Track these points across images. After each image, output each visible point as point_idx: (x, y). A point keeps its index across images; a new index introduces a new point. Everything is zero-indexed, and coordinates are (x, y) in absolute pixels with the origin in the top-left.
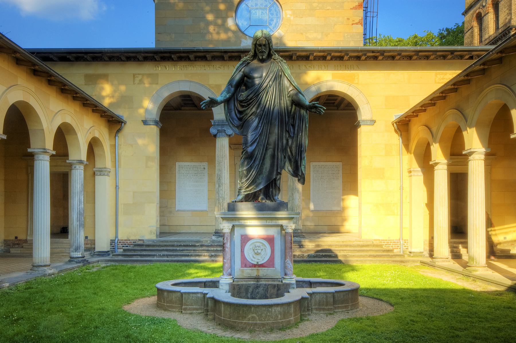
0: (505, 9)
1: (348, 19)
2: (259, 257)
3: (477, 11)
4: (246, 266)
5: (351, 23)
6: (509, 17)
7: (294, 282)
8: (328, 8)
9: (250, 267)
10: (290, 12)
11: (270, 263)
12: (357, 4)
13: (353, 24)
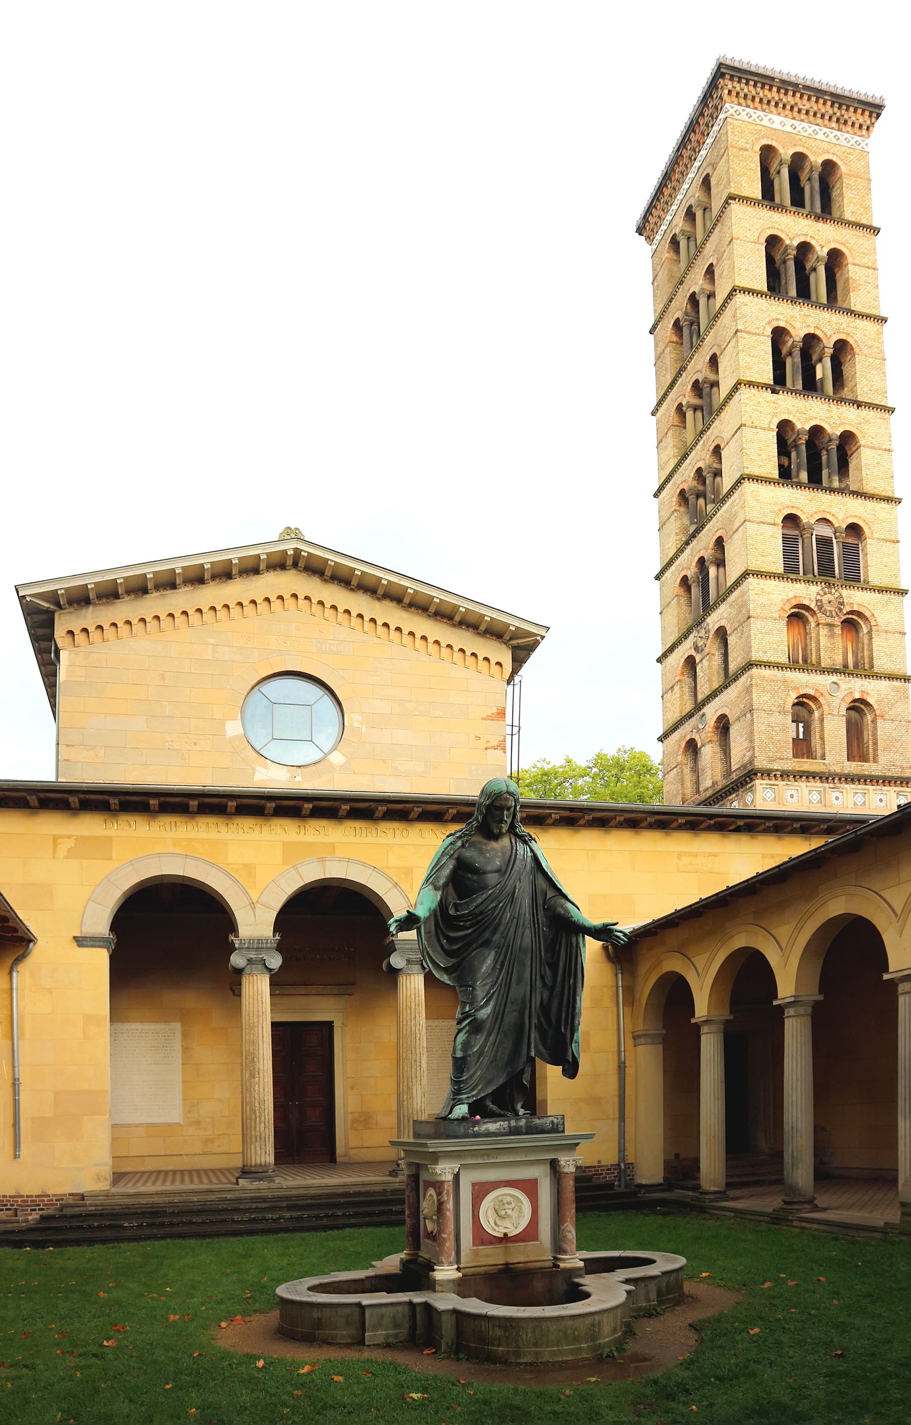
0: (743, 739)
6: (749, 754)
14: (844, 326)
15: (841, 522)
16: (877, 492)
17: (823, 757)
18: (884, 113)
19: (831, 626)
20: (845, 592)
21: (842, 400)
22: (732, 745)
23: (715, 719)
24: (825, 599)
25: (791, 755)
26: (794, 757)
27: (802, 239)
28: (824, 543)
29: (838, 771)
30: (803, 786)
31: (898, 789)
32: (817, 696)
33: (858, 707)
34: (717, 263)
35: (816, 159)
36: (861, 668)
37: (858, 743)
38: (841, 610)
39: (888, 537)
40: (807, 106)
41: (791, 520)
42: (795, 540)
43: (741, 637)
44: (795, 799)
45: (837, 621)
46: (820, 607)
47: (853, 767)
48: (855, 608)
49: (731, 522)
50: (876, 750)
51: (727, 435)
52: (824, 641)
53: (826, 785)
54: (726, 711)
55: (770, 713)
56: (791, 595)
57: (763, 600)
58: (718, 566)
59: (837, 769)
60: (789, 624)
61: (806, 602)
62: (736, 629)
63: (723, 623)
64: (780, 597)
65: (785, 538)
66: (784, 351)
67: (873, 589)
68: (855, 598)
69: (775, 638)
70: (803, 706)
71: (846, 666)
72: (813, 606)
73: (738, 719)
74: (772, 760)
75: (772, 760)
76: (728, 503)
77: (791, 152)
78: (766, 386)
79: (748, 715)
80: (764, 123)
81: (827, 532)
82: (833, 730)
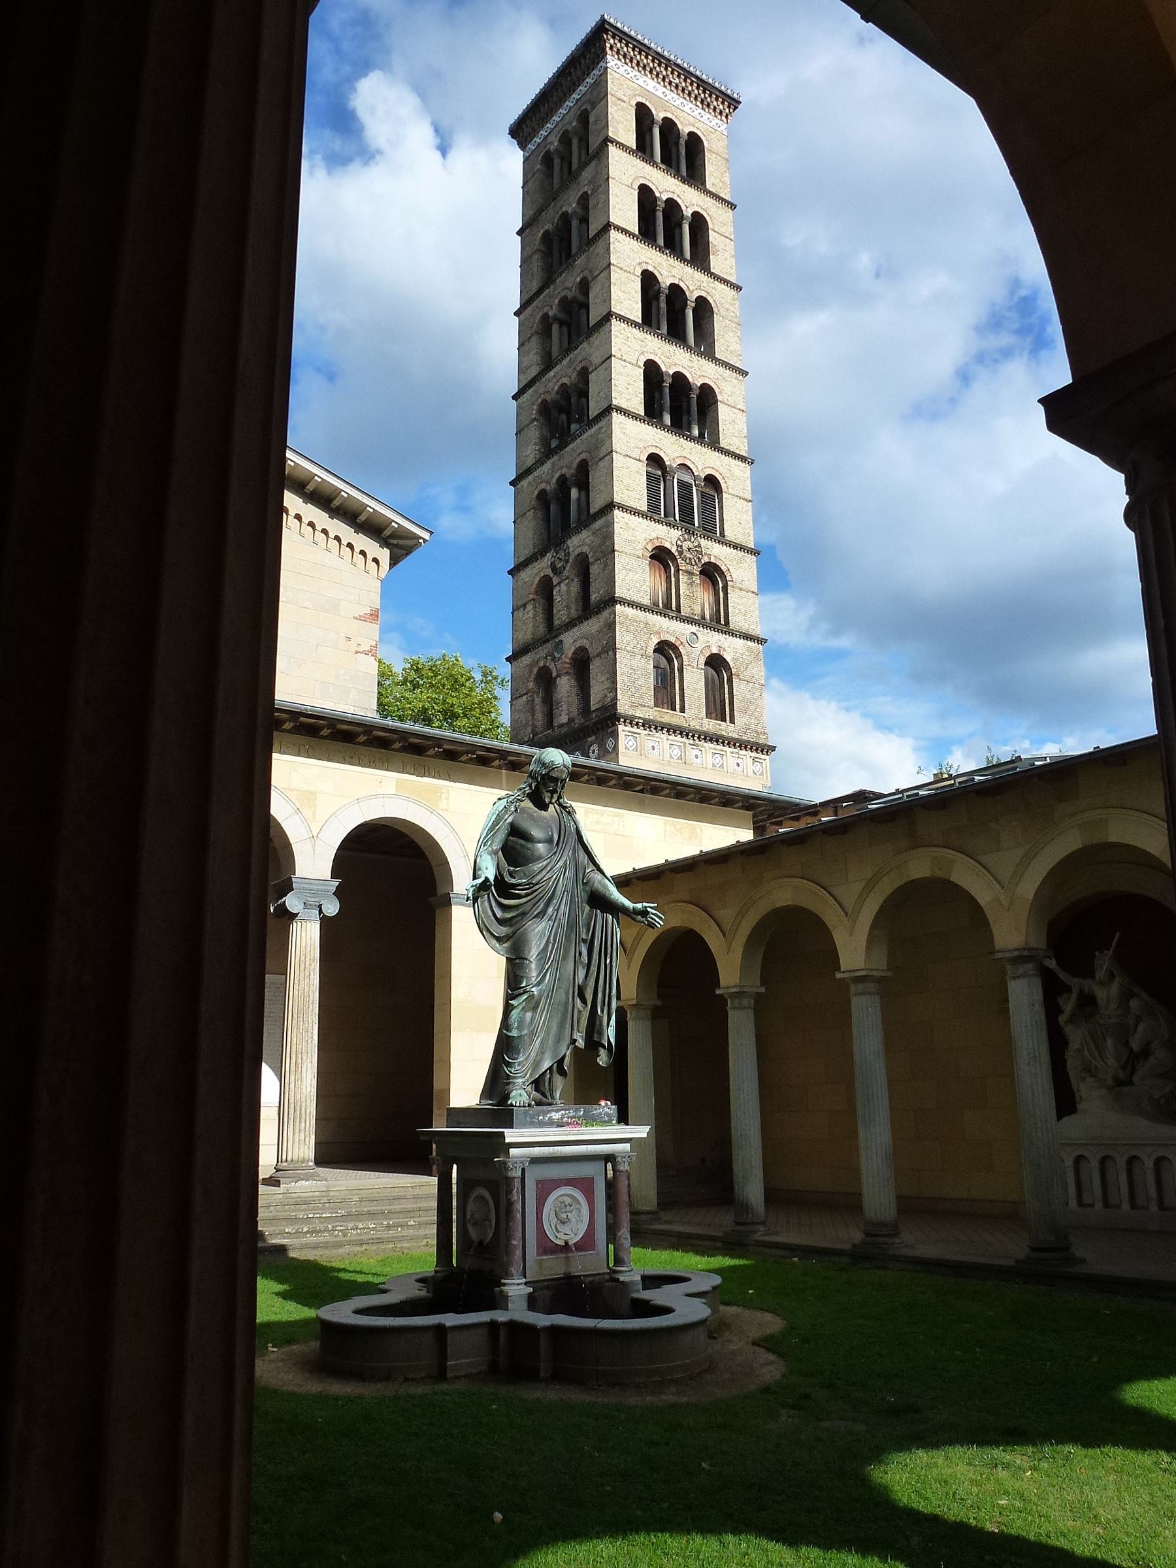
0: (604, 678)
2: (565, 1229)
3: (542, 664)
4: (545, 1253)
8: (306, 604)
11: (587, 1243)
14: (705, 284)
15: (701, 472)
16: (732, 449)
17: (683, 710)
19: (690, 573)
21: (700, 354)
23: (573, 649)
24: (686, 545)
28: (685, 487)
29: (697, 727)
30: (664, 740)
31: (754, 754)
33: (716, 663)
34: (592, 194)
35: (685, 129)
36: (719, 621)
38: (699, 559)
39: (741, 495)
40: (677, 81)
41: (655, 460)
42: (658, 480)
45: (696, 570)
46: (681, 553)
47: (711, 725)
48: (712, 560)
49: (597, 448)
51: (596, 359)
53: (685, 740)
55: (632, 654)
56: (654, 536)
57: (627, 535)
59: (695, 725)
61: (668, 545)
63: (585, 549)
64: (644, 536)
65: (649, 474)
66: (651, 293)
67: (730, 544)
69: (638, 576)
71: (703, 618)
72: (674, 550)
73: (599, 655)
74: (634, 706)
75: (634, 706)
78: (635, 324)
79: (611, 653)
80: (640, 82)
81: (688, 478)
82: (694, 681)
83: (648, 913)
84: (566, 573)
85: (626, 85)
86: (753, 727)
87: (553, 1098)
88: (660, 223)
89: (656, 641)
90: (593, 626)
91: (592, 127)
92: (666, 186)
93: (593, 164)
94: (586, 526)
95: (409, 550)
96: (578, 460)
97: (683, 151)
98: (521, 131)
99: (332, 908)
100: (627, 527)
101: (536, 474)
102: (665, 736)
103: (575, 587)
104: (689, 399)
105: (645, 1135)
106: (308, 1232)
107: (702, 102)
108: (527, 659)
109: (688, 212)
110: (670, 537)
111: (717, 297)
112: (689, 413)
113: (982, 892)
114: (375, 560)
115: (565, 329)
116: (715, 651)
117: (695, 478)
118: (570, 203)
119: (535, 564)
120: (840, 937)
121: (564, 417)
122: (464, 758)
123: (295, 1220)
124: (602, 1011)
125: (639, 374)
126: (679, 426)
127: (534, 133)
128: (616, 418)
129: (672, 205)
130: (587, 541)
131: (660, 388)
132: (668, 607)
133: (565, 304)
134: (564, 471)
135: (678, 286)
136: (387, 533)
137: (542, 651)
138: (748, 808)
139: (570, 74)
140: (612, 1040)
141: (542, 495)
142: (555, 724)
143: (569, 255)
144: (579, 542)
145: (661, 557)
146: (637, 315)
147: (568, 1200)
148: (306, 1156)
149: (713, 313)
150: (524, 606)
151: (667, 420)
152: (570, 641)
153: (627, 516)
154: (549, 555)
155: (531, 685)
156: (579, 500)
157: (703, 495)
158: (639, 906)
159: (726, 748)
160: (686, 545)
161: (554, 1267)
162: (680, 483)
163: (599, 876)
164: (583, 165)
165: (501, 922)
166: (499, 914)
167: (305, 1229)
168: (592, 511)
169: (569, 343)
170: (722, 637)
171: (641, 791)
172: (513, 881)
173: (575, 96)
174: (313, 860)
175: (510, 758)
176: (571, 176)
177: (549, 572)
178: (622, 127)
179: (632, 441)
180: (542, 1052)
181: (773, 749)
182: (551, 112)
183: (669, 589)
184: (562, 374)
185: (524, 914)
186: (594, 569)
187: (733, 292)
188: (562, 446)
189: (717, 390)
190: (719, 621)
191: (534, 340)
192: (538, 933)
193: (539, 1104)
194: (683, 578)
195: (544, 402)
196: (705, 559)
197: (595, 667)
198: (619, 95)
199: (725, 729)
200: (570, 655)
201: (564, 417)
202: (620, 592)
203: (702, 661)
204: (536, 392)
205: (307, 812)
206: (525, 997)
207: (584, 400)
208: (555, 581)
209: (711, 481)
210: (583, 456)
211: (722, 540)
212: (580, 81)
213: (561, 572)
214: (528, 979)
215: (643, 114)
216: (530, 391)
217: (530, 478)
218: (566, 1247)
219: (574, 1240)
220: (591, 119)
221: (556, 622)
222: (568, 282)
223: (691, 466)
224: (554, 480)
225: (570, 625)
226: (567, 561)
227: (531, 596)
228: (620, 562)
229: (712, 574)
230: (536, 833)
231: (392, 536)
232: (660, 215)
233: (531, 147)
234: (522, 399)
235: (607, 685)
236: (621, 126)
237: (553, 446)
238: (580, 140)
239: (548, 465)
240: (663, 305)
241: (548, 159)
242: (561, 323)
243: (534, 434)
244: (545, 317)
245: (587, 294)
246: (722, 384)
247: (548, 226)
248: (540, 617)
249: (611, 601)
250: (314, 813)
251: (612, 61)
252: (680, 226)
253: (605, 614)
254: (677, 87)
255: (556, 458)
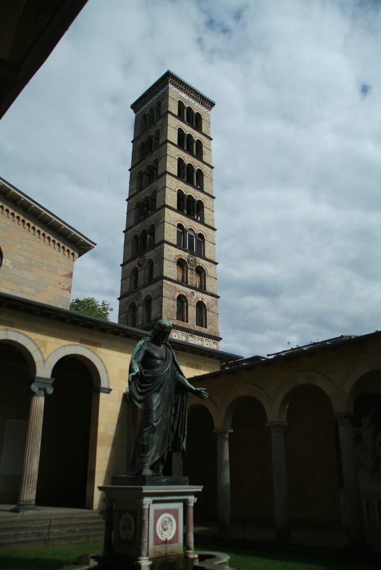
0: (157, 308)
1: (60, 284)
3: (132, 301)
5: (62, 288)
7: (196, 556)
9: (160, 544)
10: (10, 261)
11: (175, 539)
12: (68, 273)
13: (63, 289)
16: (209, 224)
17: (187, 322)
18: (215, 106)
19: (192, 269)
20: (197, 258)
21: (198, 190)
22: (152, 309)
23: (145, 296)
24: (191, 258)
25: (176, 318)
26: (177, 319)
27: (189, 133)
29: (193, 329)
31: (214, 341)
32: (186, 296)
36: (202, 289)
37: (201, 320)
41: (180, 226)
43: (159, 265)
44: (177, 337)
45: (194, 268)
46: (188, 262)
47: (197, 328)
50: (206, 323)
51: (160, 187)
52: (189, 275)
54: (150, 294)
56: (179, 254)
57: (169, 253)
58: (151, 235)
60: (177, 264)
61: (184, 258)
62: (157, 262)
63: (152, 257)
64: (175, 254)
65: (178, 231)
68: (201, 262)
69: (172, 269)
70: (182, 300)
71: (196, 286)
72: (186, 260)
76: (158, 212)
77: (187, 106)
80: (180, 94)
81: (192, 234)
82: (192, 311)
83: (202, 392)
84: (144, 266)
85: (175, 94)
86: (214, 330)
87: (159, 472)
88: (185, 142)
89: (178, 294)
90: (153, 287)
91: (162, 107)
92: (188, 130)
93: (162, 119)
94: (153, 249)
95: (86, 251)
96: (151, 224)
97: (194, 118)
98: (135, 107)
99: (50, 391)
100: (169, 250)
101: (134, 228)
102: (180, 332)
103: (147, 272)
104: (194, 205)
105: (201, 490)
106: (32, 534)
107: (202, 103)
108: (126, 299)
109: (196, 139)
110: (185, 255)
111: (205, 170)
112: (193, 210)
113: (328, 390)
114: (73, 254)
115: (148, 176)
116: (200, 300)
117: (195, 234)
118: (152, 132)
119: (131, 263)
120: (267, 408)
121: (145, 208)
122: (109, 331)
123: (22, 528)
124: (181, 435)
125: (175, 194)
126: (190, 215)
127: (140, 108)
128: (167, 210)
129: (190, 136)
130: (153, 255)
131: (183, 200)
132: (183, 282)
133: (149, 168)
134: (145, 227)
135: (191, 165)
136: (79, 243)
137: (132, 296)
138: (218, 359)
139: (155, 89)
140: (185, 447)
141: (136, 237)
142: (136, 325)
143: (151, 151)
144: (150, 255)
145: (181, 263)
146: (176, 173)
147: (167, 520)
148: (32, 499)
149: (203, 175)
150: (126, 278)
151: (185, 212)
152: (144, 292)
153: (169, 246)
154: (137, 259)
155: (127, 309)
156: (150, 239)
157: (198, 241)
158: (199, 389)
159: (203, 338)
160: (191, 258)
161: (161, 549)
162: (189, 234)
163: (181, 376)
164: (158, 120)
165: (140, 394)
166: (139, 390)
167: (30, 533)
168: (155, 243)
169: (149, 181)
170: (203, 295)
171: (178, 350)
172: (146, 375)
173: (156, 96)
174: (44, 371)
175: (127, 333)
176: (153, 122)
177: (137, 266)
178: (173, 108)
179: (172, 219)
180: (156, 452)
181: (221, 339)
182: (147, 101)
183: (183, 275)
184: (146, 192)
185: (150, 390)
186: (155, 265)
187: (210, 169)
188: (145, 219)
189: (204, 203)
190: (202, 289)
191: (136, 180)
192: (156, 399)
193: (156, 475)
194: (189, 271)
195: (138, 202)
196: (198, 265)
197: (154, 303)
198: (173, 97)
199: (203, 330)
200: (144, 297)
201: (145, 208)
202: (165, 274)
203: (195, 303)
204: (135, 198)
205: (43, 350)
206: (150, 427)
207: (154, 203)
208: (139, 269)
209: (201, 236)
210: (153, 223)
211: (204, 258)
212: (158, 91)
213: (142, 266)
214: (152, 419)
215: (181, 104)
216: (133, 198)
217: (131, 230)
218: (166, 542)
219: (169, 538)
220: (162, 104)
221: (139, 285)
222: (150, 160)
223: (194, 230)
224: (141, 231)
225: (144, 286)
226: (144, 262)
227: (129, 275)
228: (166, 263)
229: (200, 271)
230: (157, 355)
231: (80, 245)
232: (185, 140)
233: (139, 112)
234: (131, 201)
235: (158, 310)
236: (172, 108)
237: (141, 218)
238: (158, 111)
239: (138, 226)
240: (185, 171)
241: (145, 117)
242: (147, 174)
243: (133, 214)
244: (141, 172)
245: (157, 165)
246: (206, 201)
247: (143, 140)
248: (132, 283)
249: (162, 277)
250: (45, 351)
251: (170, 86)
252: (193, 144)
253: (159, 282)
254: (193, 97)
255: (142, 223)
